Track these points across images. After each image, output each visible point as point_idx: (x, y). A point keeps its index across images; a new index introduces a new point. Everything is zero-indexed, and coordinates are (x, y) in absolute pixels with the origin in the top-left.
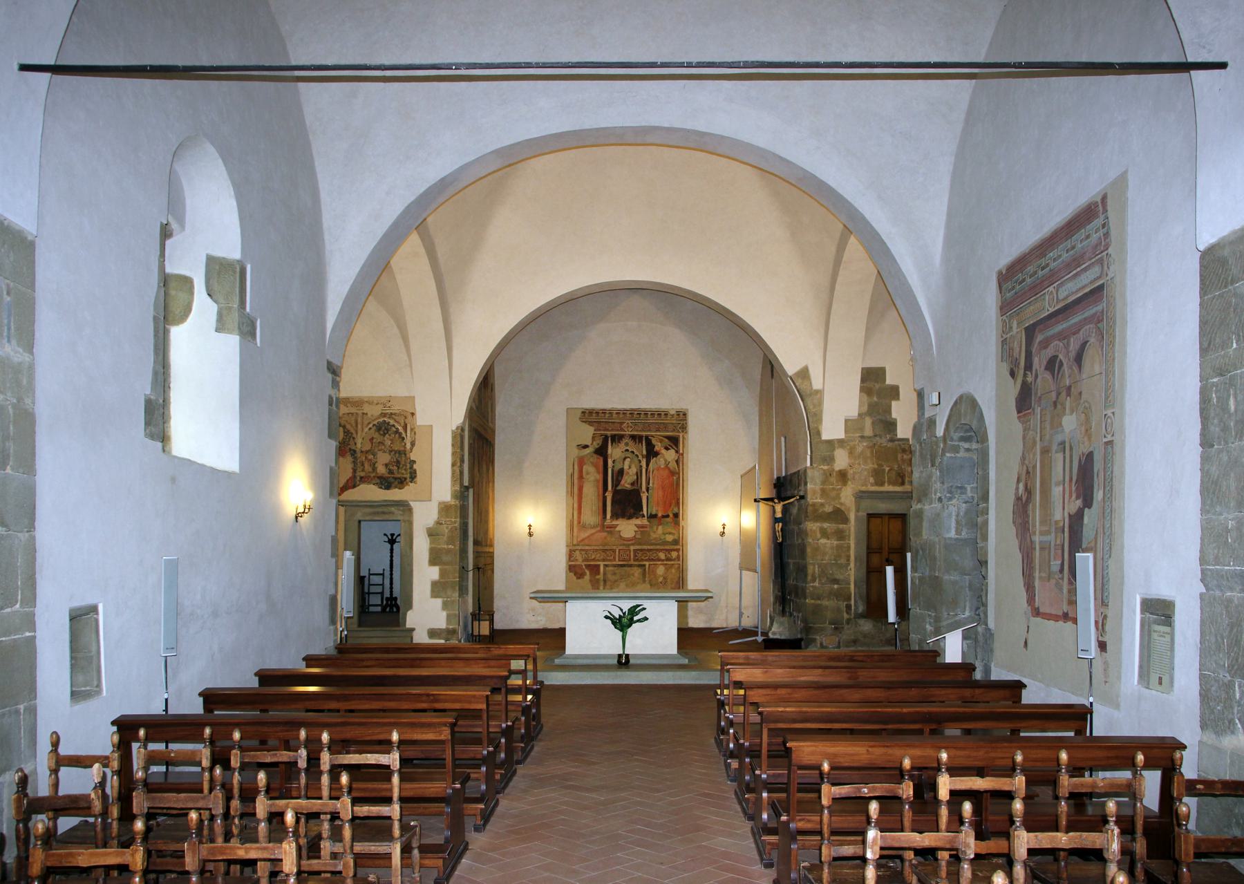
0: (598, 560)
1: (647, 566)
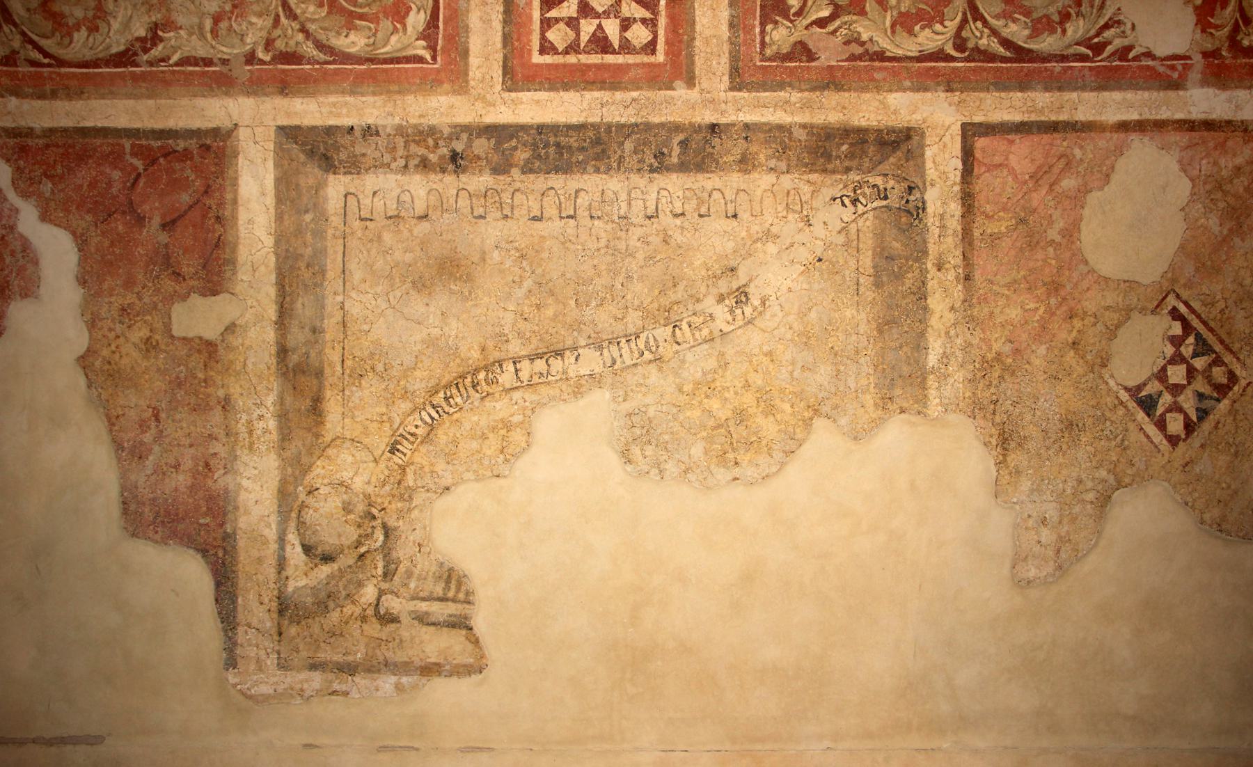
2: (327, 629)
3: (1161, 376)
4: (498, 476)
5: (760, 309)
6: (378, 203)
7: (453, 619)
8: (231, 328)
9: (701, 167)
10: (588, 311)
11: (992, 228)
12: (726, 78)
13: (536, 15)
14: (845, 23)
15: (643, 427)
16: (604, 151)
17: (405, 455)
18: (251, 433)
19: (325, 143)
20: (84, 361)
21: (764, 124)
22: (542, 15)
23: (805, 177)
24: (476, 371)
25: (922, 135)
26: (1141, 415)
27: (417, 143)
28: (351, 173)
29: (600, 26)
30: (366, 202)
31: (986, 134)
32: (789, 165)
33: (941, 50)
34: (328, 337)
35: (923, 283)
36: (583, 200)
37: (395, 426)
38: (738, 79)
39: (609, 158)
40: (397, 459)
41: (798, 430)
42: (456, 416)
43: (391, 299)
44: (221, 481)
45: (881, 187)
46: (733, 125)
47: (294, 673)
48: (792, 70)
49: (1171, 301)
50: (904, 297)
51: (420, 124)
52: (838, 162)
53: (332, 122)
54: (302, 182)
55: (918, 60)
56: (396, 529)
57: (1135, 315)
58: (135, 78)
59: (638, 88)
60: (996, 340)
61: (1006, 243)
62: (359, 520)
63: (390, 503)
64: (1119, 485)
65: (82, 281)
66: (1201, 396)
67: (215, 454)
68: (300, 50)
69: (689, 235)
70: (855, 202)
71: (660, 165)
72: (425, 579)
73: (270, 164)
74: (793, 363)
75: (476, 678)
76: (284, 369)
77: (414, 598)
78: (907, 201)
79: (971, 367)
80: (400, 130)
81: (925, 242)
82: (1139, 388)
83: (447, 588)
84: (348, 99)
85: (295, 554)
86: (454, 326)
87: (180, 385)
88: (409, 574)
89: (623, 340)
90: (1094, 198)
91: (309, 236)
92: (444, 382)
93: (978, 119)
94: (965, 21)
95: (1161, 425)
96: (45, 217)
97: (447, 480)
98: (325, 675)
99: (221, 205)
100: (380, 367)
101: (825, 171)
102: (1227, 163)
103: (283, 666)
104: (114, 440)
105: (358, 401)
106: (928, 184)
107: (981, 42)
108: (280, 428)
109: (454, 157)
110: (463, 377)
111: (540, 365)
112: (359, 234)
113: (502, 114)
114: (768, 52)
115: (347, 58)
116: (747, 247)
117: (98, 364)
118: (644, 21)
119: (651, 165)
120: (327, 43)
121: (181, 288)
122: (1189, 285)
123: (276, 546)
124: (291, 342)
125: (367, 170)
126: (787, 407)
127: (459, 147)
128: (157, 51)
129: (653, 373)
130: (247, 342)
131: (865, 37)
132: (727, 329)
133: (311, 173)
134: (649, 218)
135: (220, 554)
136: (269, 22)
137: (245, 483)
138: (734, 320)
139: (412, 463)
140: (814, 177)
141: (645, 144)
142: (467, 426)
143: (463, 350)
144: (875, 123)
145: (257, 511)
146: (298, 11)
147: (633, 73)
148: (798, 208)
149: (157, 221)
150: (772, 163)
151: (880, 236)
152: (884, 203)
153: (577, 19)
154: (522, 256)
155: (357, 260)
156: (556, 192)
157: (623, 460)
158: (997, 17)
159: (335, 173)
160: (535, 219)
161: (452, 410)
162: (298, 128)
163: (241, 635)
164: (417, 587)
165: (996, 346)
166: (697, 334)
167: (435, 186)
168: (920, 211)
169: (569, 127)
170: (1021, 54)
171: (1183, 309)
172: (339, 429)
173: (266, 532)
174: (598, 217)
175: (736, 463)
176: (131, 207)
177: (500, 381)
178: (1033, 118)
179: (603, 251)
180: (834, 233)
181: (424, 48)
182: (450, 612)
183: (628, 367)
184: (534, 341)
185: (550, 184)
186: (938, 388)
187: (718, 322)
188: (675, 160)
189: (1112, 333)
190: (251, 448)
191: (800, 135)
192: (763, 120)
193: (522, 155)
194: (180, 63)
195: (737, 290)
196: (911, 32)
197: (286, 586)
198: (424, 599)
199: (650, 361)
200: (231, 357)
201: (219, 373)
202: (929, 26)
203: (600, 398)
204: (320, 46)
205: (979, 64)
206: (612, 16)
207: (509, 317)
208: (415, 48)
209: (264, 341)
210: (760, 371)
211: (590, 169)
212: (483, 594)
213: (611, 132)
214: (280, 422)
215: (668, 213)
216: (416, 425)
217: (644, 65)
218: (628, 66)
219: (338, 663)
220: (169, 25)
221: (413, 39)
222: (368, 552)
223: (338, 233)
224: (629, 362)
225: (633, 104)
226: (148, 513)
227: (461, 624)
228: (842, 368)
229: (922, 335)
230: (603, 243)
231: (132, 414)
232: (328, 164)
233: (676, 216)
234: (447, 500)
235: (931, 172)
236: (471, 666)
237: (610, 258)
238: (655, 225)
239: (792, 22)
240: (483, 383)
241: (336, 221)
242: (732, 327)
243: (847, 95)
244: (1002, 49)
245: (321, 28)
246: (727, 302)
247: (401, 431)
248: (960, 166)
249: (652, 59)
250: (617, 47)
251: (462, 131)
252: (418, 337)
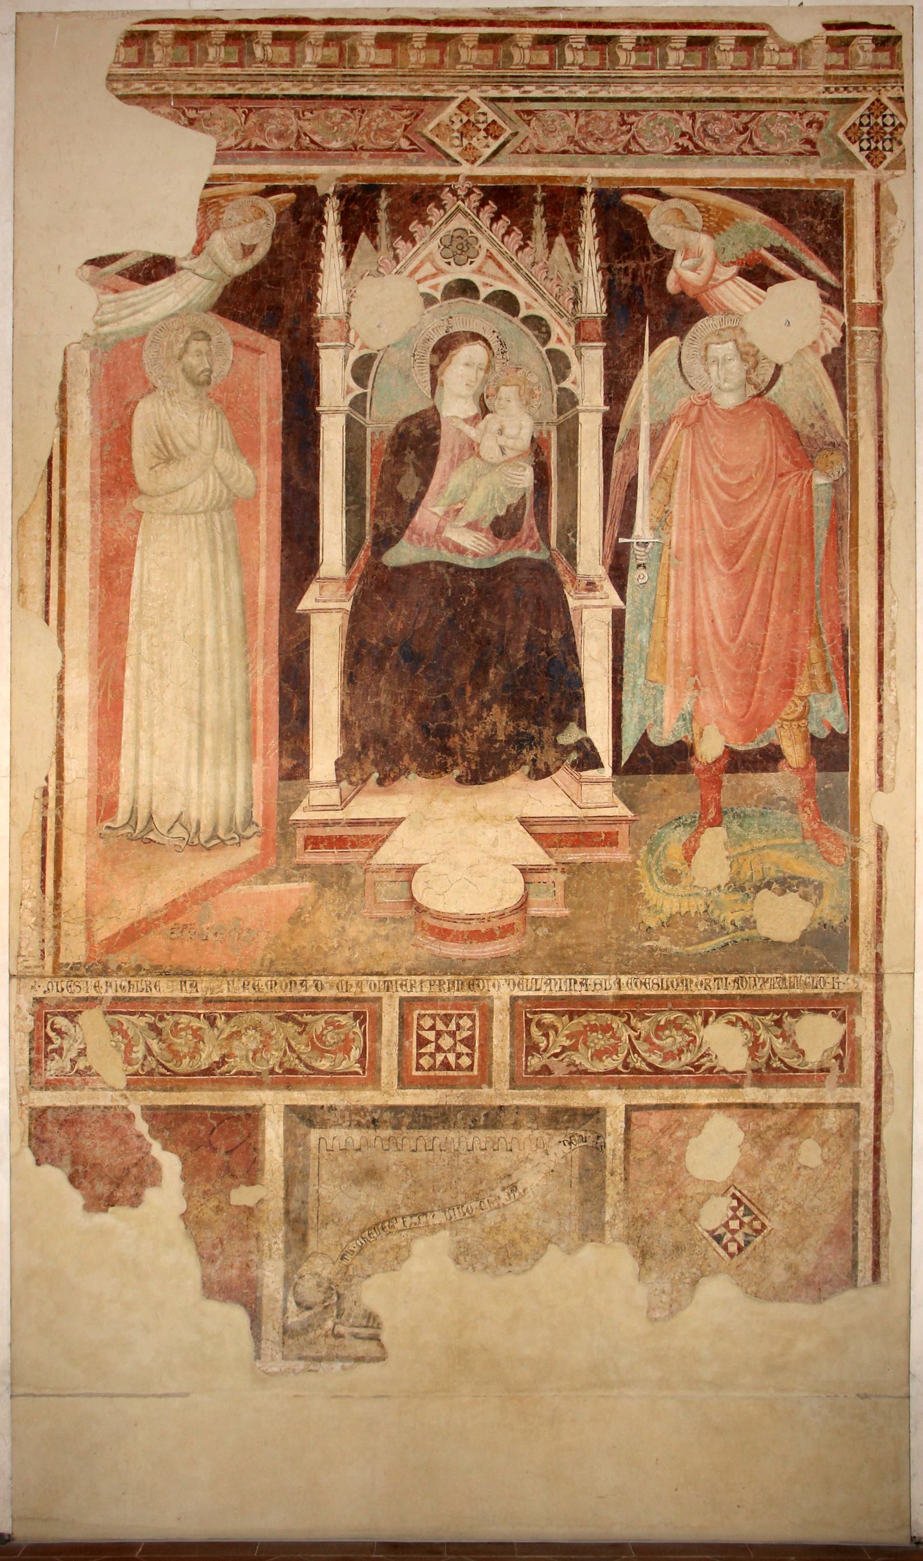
0: (254, 1080)
1: (615, 1123)
3: (726, 1225)
6: (336, 1143)
8: (261, 1201)
11: (639, 1155)
13: (414, 1051)
20: (184, 1216)
24: (384, 1222)
26: (715, 1244)
30: (330, 1142)
36: (437, 1142)
38: (514, 1083)
40: (345, 1262)
44: (254, 1272)
48: (540, 1079)
49: (732, 1190)
53: (313, 1103)
54: (298, 1132)
55: (604, 1073)
57: (713, 1197)
58: (213, 1081)
61: (647, 1163)
64: (703, 1275)
65: (183, 1178)
66: (746, 1235)
70: (570, 1143)
71: (475, 1125)
75: (381, 1363)
77: (352, 1326)
80: (347, 1108)
82: (714, 1231)
85: (292, 1306)
86: (373, 1201)
87: (234, 1228)
88: (349, 1315)
90: (692, 1142)
93: (633, 1103)
94: (629, 1053)
95: (725, 1248)
96: (165, 1148)
97: (370, 1272)
99: (256, 1142)
101: (556, 1129)
102: (763, 1124)
104: (199, 1253)
108: (285, 1247)
109: (374, 1121)
110: (377, 1224)
111: (415, 1219)
113: (397, 1101)
115: (321, 1072)
117: (191, 1218)
118: (467, 1054)
121: (236, 1182)
122: (742, 1183)
127: (376, 1116)
128: (224, 1068)
131: (577, 1062)
133: (302, 1129)
140: (550, 1131)
142: (379, 1247)
143: (378, 1212)
145: (272, 1287)
147: (462, 1080)
149: (223, 1150)
151: (582, 1159)
158: (645, 1052)
163: (263, 1345)
169: (430, 1107)
170: (657, 1070)
171: (738, 1194)
176: (210, 1143)
178: (662, 1102)
188: (482, 1123)
189: (701, 1205)
191: (544, 1111)
193: (407, 1120)
194: (237, 1073)
196: (601, 1060)
203: (445, 1234)
204: (307, 1066)
207: (400, 1197)
212: (386, 1324)
220: (230, 1055)
226: (216, 1287)
227: (375, 1338)
229: (603, 1206)
231: (209, 1242)
232: (311, 1124)
234: (368, 1282)
235: (609, 1128)
241: (315, 1151)
252: (355, 1206)
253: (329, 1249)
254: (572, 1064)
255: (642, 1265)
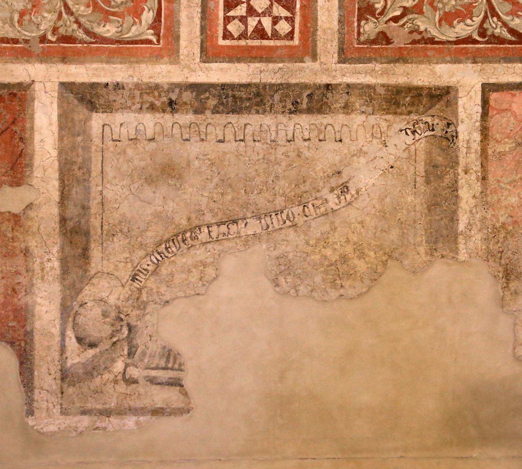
2: (92, 388)
4: (198, 294)
5: (356, 196)
6: (124, 130)
7: (171, 380)
8: (30, 206)
9: (320, 111)
10: (252, 197)
11: (500, 148)
12: (336, 55)
13: (221, 14)
14: (410, 19)
15: (285, 265)
16: (262, 101)
17: (141, 282)
18: (43, 270)
19: (91, 93)
21: (359, 84)
22: (225, 14)
23: (383, 117)
24: (185, 232)
25: (457, 91)
27: (148, 94)
28: (106, 112)
29: (260, 22)
30: (116, 130)
31: (497, 91)
32: (374, 110)
33: (470, 37)
34: (93, 211)
35: (456, 181)
36: (249, 130)
37: (135, 265)
39: (265, 105)
40: (136, 284)
41: (379, 267)
42: (172, 259)
43: (132, 189)
44: (22, 300)
45: (430, 123)
46: (340, 85)
47: (71, 417)
50: (444, 190)
51: (150, 82)
52: (404, 108)
53: (95, 80)
56: (136, 326)
59: (283, 62)
60: (502, 215)
62: (112, 321)
63: (132, 311)
67: (19, 283)
68: (75, 35)
69: (313, 152)
70: (414, 132)
71: (296, 110)
72: (154, 356)
73: (55, 106)
74: (376, 228)
75: (185, 416)
76: (65, 231)
77: (147, 368)
78: (447, 132)
79: (486, 232)
80: (137, 86)
81: (457, 157)
83: (168, 361)
84: (105, 65)
85: (72, 343)
86: (171, 205)
88: (144, 354)
89: (274, 214)
91: (80, 151)
92: (165, 238)
93: (492, 81)
94: (486, 17)
98: (91, 418)
99: (23, 130)
100: (125, 230)
101: (395, 113)
103: (64, 412)
105: (111, 250)
106: (459, 121)
107: (496, 31)
109: (171, 103)
110: (177, 235)
111: (223, 228)
112: (112, 149)
114: (362, 39)
116: (348, 159)
118: (286, 18)
119: (290, 110)
120: (92, 30)
123: (59, 339)
124: (68, 215)
125: (117, 111)
126: (372, 254)
127: (174, 97)
129: (291, 234)
130: (40, 215)
131: (422, 28)
132: (335, 208)
133: (81, 112)
134: (289, 141)
135: (23, 344)
136: (55, 16)
137: (39, 300)
138: (340, 202)
139: (146, 287)
140: (389, 117)
141: (286, 96)
143: (177, 219)
144: (427, 84)
145: (47, 317)
146: (74, 10)
147: (279, 52)
148: (379, 136)
150: (364, 108)
151: (429, 153)
152: (432, 133)
153: (246, 17)
154: (212, 164)
155: (111, 165)
156: (233, 125)
157: (274, 284)
158: (507, 14)
159: (96, 112)
160: (220, 141)
161: (170, 255)
162: (73, 84)
164: (149, 361)
165: (502, 219)
166: (318, 211)
167: (159, 121)
168: (455, 138)
172: (100, 267)
173: (53, 330)
174: (258, 141)
175: (342, 286)
177: (199, 237)
179: (261, 161)
180: (401, 151)
181: (152, 35)
182: (169, 376)
183: (276, 230)
184: (220, 214)
185: (229, 120)
186: (465, 244)
187: (330, 203)
188: (304, 106)
190: (42, 278)
191: (381, 91)
192: (358, 81)
193: (212, 102)
195: (342, 185)
196: (451, 25)
197: (66, 363)
198: (153, 369)
199: (290, 227)
200: (30, 223)
201: (22, 233)
202: (463, 21)
204: (87, 32)
205: (495, 46)
206: (267, 15)
207: (205, 200)
208: (147, 35)
209: (51, 214)
210: (356, 232)
211: (253, 111)
212: (189, 365)
213: (266, 89)
214: (62, 263)
215: (300, 139)
216: (148, 264)
217: (286, 47)
218: (277, 47)
219: (99, 410)
221: (146, 29)
222: (118, 341)
223: (98, 149)
224: (277, 227)
225: (280, 72)
228: (406, 231)
230: (261, 156)
232: (93, 107)
233: (305, 140)
234: (168, 309)
235: (462, 114)
236: (183, 409)
237: (265, 166)
238: (291, 147)
239: (377, 19)
240: (189, 239)
241: (97, 141)
242: (339, 207)
243: (410, 65)
244: (509, 36)
245: (88, 21)
246: (336, 192)
247: (138, 268)
248: (480, 110)
249: (291, 43)
250: (270, 35)
251: (176, 87)
253: (116, 268)
254: (415, 30)
255: (506, 287)
